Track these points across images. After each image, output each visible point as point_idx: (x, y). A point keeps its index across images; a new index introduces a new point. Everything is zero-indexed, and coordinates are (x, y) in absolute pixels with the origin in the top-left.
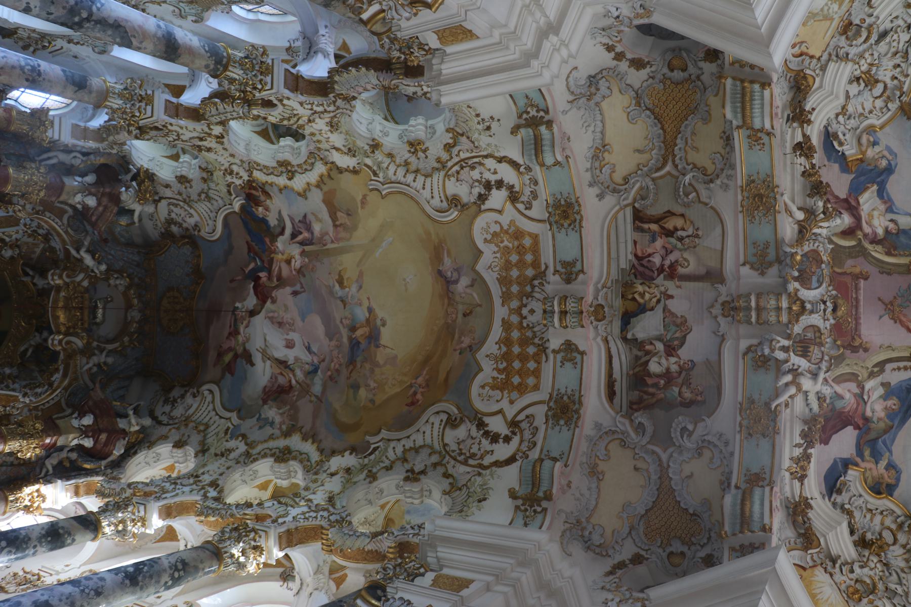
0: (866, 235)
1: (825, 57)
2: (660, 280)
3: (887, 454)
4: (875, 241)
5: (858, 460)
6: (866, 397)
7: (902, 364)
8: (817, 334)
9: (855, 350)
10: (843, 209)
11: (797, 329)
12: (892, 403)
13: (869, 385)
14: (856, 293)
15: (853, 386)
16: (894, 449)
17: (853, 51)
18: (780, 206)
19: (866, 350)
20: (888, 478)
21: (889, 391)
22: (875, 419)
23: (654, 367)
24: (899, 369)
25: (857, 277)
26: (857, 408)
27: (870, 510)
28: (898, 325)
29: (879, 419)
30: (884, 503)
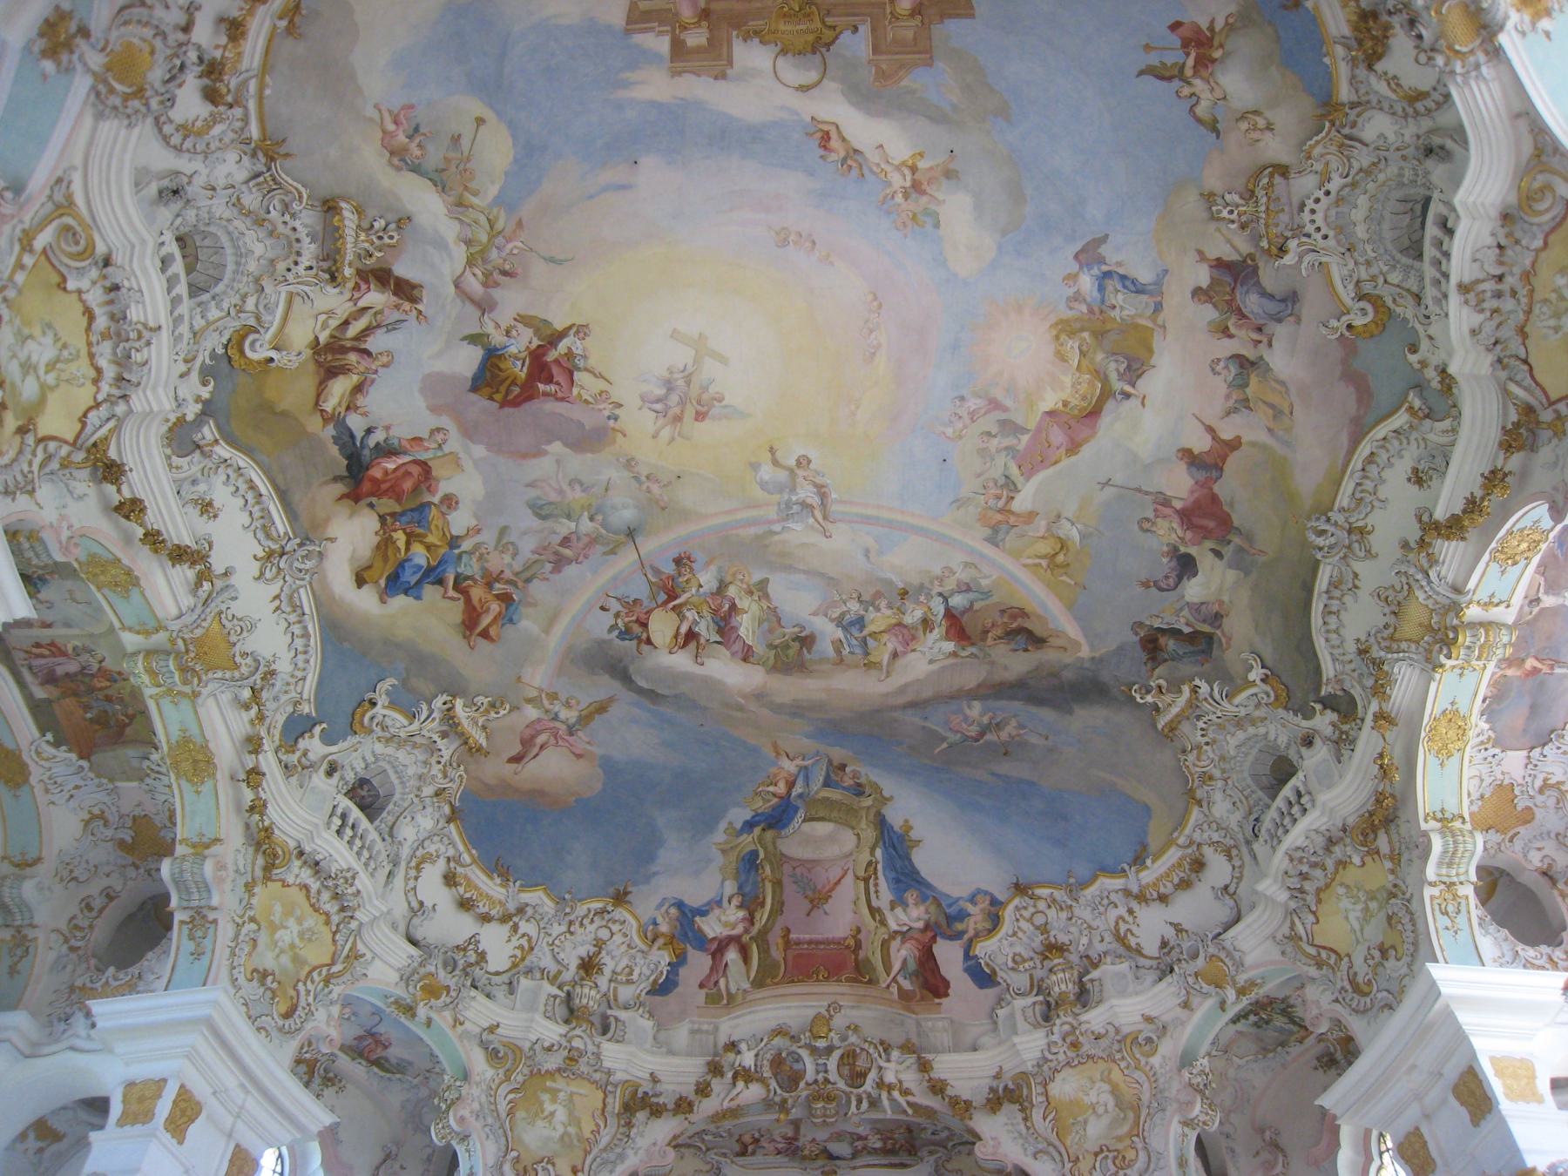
0: (746, 931)
1: (597, 1076)
2: (800, 1144)
3: (961, 902)
4: (751, 920)
5: (966, 937)
6: (905, 928)
7: (872, 889)
8: (845, 1061)
9: (858, 945)
10: (721, 960)
11: (841, 1085)
12: (910, 897)
13: (894, 926)
14: (803, 943)
15: (895, 944)
16: (955, 892)
17: (591, 1048)
18: (734, 1104)
19: (859, 930)
20: (984, 904)
21: (899, 902)
22: (926, 917)
23: (878, 1145)
24: (877, 892)
25: (788, 943)
26: (916, 940)
27: (1015, 934)
28: (833, 894)
29: (927, 912)
30: (1008, 914)
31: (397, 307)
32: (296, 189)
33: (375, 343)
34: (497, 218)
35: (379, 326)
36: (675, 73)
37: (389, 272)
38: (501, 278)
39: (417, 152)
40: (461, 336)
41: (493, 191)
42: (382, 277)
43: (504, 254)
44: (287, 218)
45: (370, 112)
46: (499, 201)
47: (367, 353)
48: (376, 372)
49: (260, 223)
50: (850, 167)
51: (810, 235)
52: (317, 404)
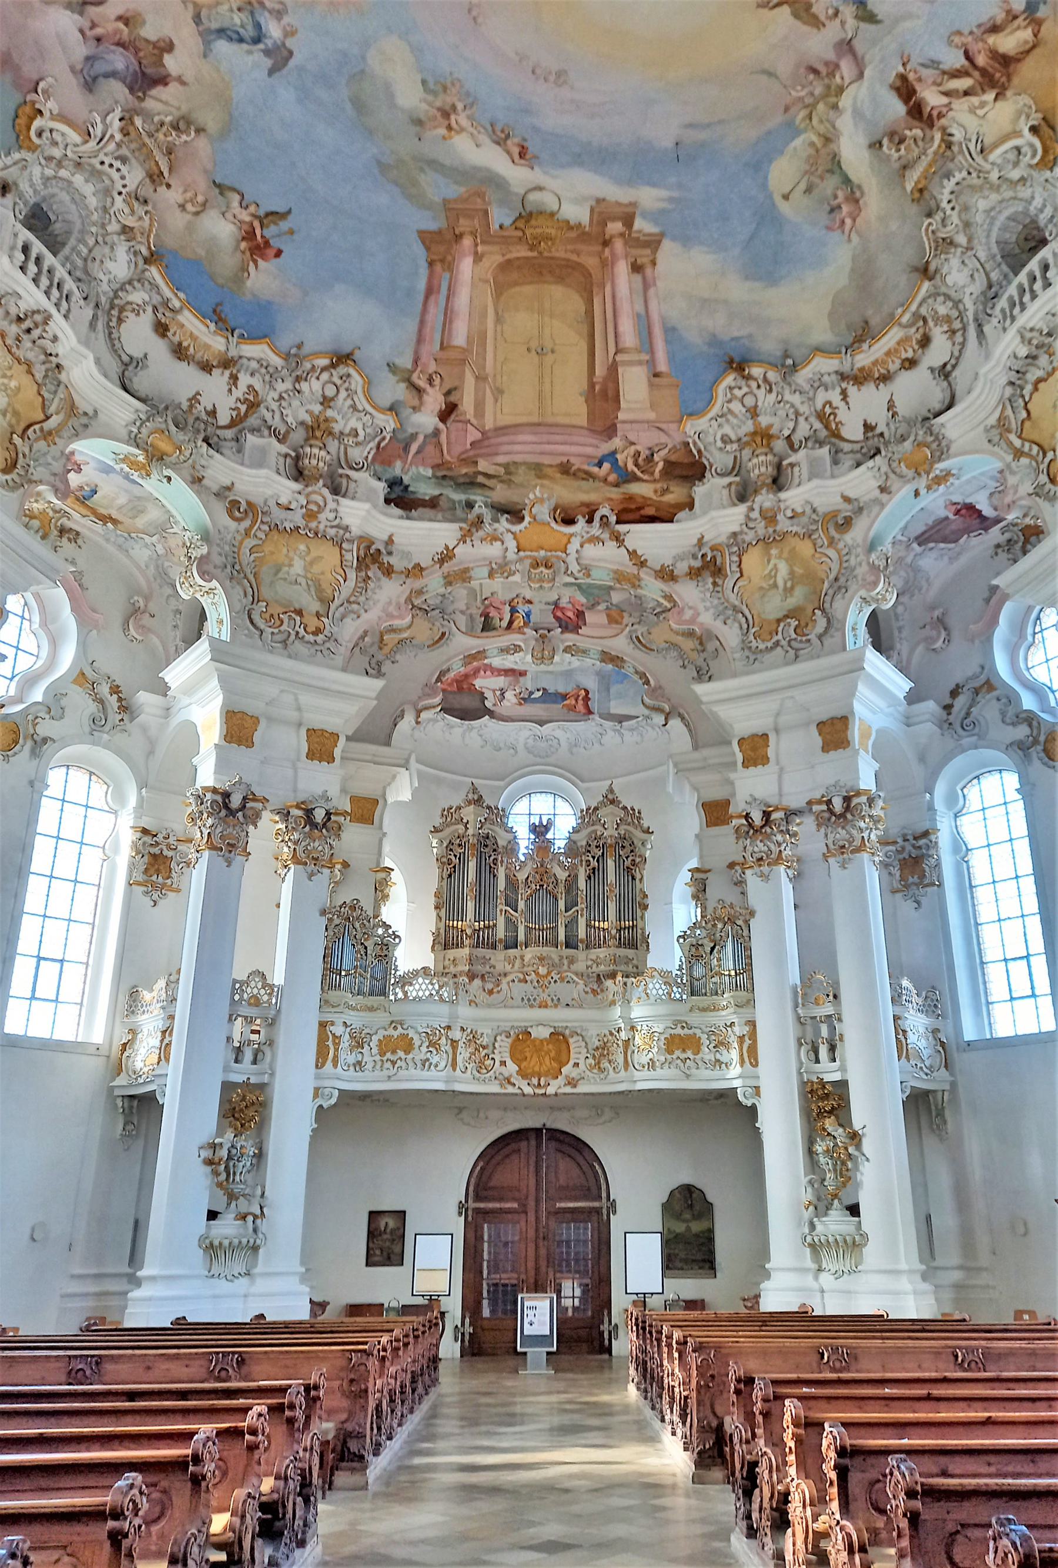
31: (920, 80)
32: (927, 234)
33: (958, 61)
34: (803, 119)
35: (944, 73)
36: (634, 204)
37: (909, 113)
38: (823, 70)
39: (841, 194)
40: (879, 26)
41: (798, 142)
42: (917, 111)
43: (811, 88)
44: (949, 212)
45: (855, 237)
46: (797, 132)
47: (968, 56)
48: (971, 33)
49: (967, 225)
50: (502, 131)
51: (537, 79)
52: (1034, 47)
